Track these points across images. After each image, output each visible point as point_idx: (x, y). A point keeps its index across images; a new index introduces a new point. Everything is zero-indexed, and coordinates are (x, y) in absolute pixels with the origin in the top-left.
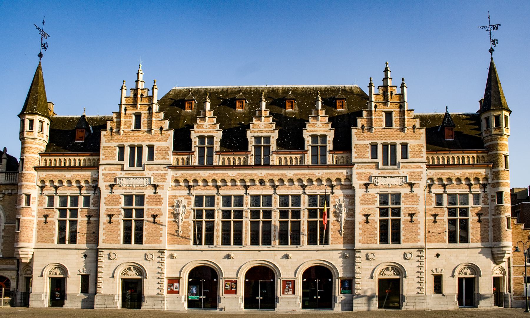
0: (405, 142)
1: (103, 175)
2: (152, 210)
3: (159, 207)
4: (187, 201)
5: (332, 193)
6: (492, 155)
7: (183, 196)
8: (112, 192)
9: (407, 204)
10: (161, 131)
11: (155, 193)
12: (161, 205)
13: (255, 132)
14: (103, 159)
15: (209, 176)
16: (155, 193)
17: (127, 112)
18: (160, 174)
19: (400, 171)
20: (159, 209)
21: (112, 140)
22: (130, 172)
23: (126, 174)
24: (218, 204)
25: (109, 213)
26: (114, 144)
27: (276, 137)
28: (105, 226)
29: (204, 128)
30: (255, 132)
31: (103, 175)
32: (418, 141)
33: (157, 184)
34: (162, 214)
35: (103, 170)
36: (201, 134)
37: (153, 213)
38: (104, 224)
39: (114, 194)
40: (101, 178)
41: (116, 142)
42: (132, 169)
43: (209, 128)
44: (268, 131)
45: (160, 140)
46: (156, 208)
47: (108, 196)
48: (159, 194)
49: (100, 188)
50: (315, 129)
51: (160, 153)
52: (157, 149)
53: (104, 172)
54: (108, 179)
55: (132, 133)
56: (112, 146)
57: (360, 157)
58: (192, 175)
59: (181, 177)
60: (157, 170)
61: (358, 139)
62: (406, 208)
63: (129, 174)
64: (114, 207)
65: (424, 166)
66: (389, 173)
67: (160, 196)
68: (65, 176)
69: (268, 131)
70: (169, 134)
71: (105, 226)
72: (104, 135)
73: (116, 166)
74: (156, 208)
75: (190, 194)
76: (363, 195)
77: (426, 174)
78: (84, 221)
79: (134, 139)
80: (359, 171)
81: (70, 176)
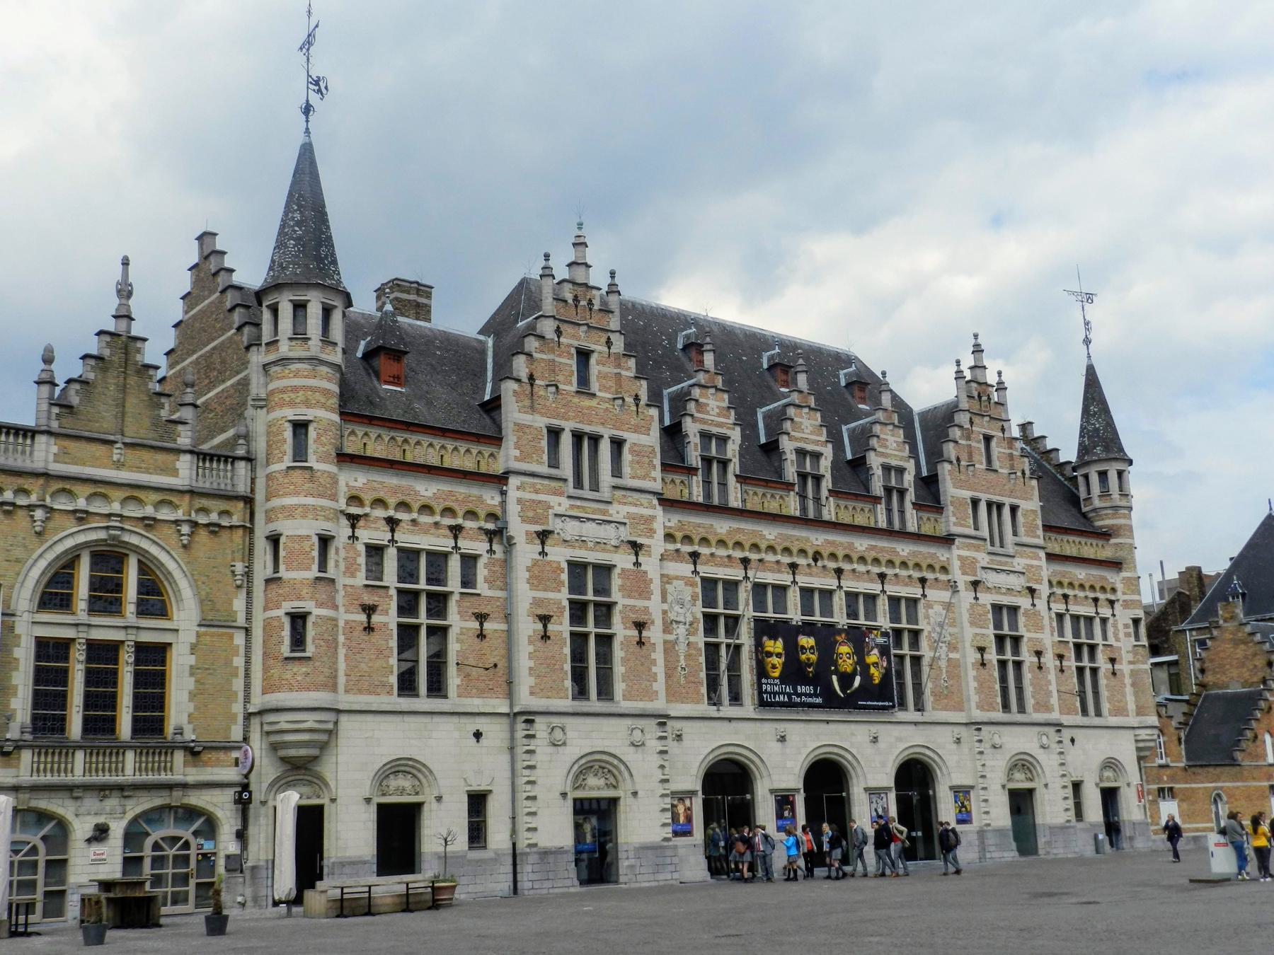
0: (1015, 501)
1: (519, 501)
2: (632, 608)
3: (646, 603)
4: (689, 590)
5: (924, 596)
6: (1117, 544)
7: (682, 578)
8: (543, 553)
9: (1029, 631)
10: (637, 405)
11: (637, 564)
12: (649, 599)
13: (797, 439)
14: (516, 459)
15: (729, 532)
16: (637, 564)
17: (562, 339)
18: (642, 516)
19: (1017, 560)
20: (647, 608)
21: (532, 409)
22: (578, 503)
23: (572, 507)
24: (747, 604)
25: (540, 612)
26: (541, 422)
27: (830, 458)
28: (531, 649)
29: (708, 413)
30: (797, 439)
31: (519, 501)
32: (1031, 504)
33: (640, 540)
34: (653, 623)
35: (518, 488)
36: (706, 427)
37: (634, 617)
38: (530, 642)
39: (549, 558)
40: (513, 509)
41: (542, 415)
42: (579, 493)
43: (719, 415)
44: (817, 442)
45: (636, 430)
46: (640, 603)
47: (535, 563)
48: (643, 568)
49: (510, 538)
50: (888, 451)
51: (638, 463)
52: (632, 451)
53: (519, 494)
54: (531, 514)
55: (576, 400)
56: (536, 425)
57: (962, 525)
58: (699, 525)
59: (679, 530)
60: (636, 505)
61: (955, 487)
62: (1030, 639)
63: (578, 507)
64: (551, 595)
65: (1042, 554)
66: (1001, 563)
67: (645, 572)
68: (417, 493)
69: (817, 442)
70: (652, 417)
71: (531, 649)
72: (515, 391)
73: (546, 482)
74: (640, 603)
75: (695, 572)
76: (972, 606)
77: (1047, 571)
78: (468, 629)
79: (581, 414)
80: (965, 553)
81: (429, 494)
